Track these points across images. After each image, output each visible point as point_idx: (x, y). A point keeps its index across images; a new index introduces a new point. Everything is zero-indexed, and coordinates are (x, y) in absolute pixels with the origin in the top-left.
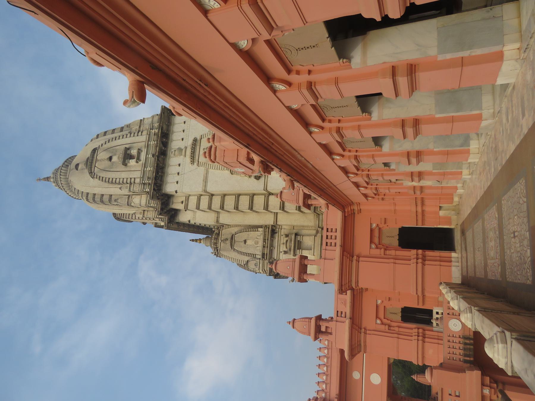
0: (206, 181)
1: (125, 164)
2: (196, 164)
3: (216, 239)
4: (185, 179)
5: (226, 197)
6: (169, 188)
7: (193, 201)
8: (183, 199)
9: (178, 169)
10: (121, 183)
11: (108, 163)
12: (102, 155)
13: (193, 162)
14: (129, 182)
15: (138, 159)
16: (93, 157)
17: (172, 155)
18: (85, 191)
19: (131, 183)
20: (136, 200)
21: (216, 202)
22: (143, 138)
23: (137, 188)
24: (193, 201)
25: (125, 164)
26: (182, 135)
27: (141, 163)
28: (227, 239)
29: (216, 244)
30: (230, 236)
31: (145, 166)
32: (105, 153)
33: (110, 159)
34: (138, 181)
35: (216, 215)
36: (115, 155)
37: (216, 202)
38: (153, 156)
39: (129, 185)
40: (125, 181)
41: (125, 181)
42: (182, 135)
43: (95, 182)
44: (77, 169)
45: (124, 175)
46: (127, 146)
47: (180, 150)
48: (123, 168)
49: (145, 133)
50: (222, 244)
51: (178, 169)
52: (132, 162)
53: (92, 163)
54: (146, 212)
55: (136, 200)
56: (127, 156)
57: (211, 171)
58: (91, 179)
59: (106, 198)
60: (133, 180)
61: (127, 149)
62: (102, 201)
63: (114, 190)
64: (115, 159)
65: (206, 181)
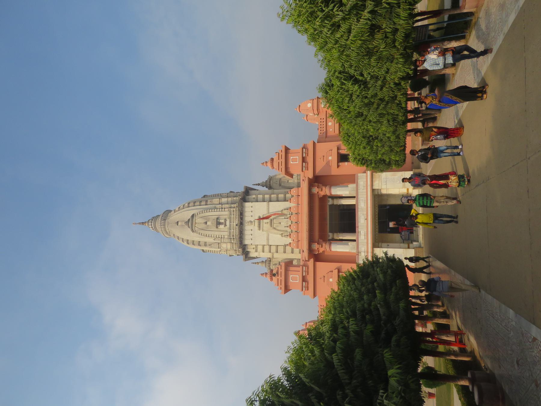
0: (268, 239)
1: (217, 227)
2: (261, 230)
3: (270, 264)
4: (255, 237)
6: (247, 242)
7: (260, 248)
8: (254, 247)
9: (251, 232)
10: (216, 238)
11: (204, 225)
12: (198, 220)
13: (259, 229)
14: (220, 237)
15: (225, 225)
16: (192, 221)
17: (246, 224)
18: (185, 238)
20: (224, 246)
21: (273, 249)
22: (227, 213)
23: (226, 241)
24: (260, 248)
25: (217, 227)
26: (251, 214)
28: (276, 264)
29: (269, 266)
30: (277, 263)
31: (230, 229)
32: (201, 219)
33: (206, 223)
34: (227, 237)
37: (273, 249)
38: (237, 225)
40: (218, 236)
41: (218, 236)
42: (251, 214)
43: (195, 234)
45: (217, 233)
46: (217, 217)
47: (251, 222)
48: (217, 230)
50: (273, 267)
51: (251, 232)
52: (222, 227)
53: (192, 224)
55: (224, 246)
56: (218, 223)
57: (270, 234)
60: (223, 236)
61: (217, 219)
62: (199, 245)
63: (210, 240)
64: (209, 223)
65: (268, 239)
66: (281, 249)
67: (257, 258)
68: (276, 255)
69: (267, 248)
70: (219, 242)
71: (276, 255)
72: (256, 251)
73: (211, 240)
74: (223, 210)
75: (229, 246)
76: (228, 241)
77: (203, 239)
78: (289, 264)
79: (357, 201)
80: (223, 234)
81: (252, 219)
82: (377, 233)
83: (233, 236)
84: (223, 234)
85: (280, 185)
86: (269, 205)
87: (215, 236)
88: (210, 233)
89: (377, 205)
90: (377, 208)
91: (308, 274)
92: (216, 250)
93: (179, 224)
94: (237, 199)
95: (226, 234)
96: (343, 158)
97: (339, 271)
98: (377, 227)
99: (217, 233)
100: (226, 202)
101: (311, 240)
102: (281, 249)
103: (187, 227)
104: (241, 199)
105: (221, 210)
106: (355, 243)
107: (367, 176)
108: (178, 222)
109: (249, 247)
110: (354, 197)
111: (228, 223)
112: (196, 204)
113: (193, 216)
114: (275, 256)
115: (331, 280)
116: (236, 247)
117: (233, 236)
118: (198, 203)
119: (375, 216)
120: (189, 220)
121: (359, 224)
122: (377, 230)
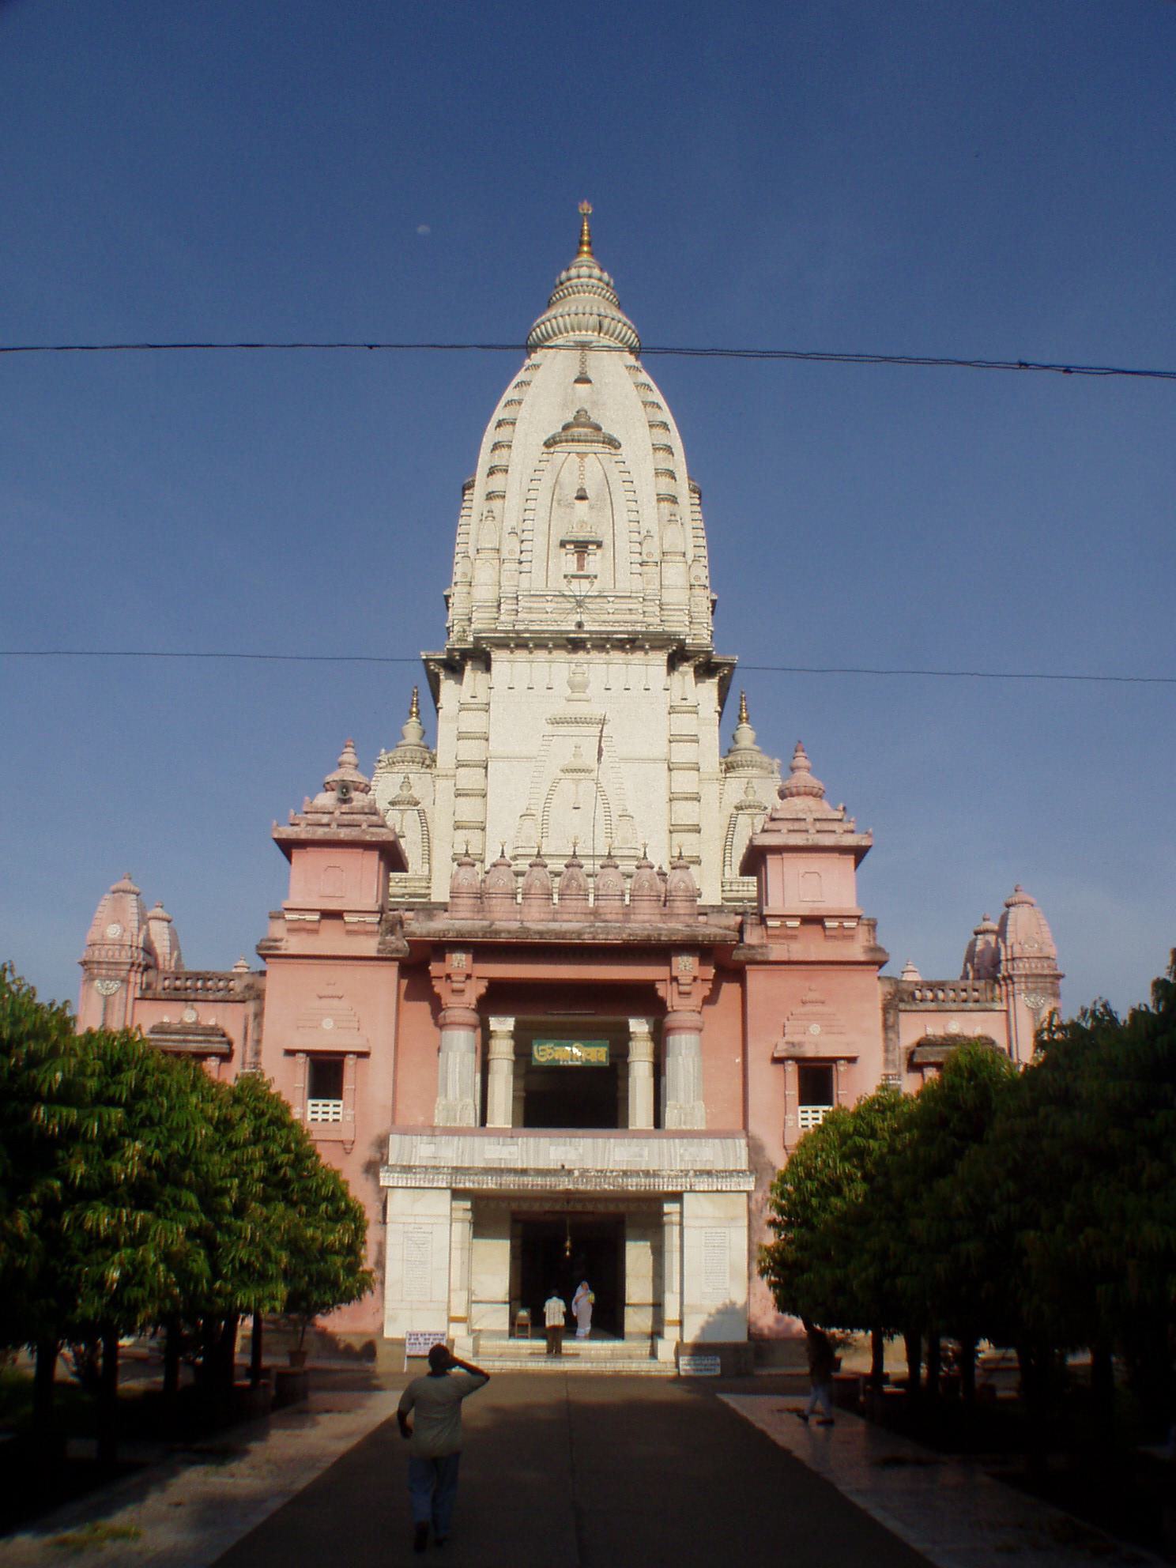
1: (563, 544)
2: (550, 729)
5: (479, 800)
7: (472, 722)
12: (594, 466)
13: (555, 722)
19: (521, 563)
21: (469, 778)
24: (472, 722)
27: (563, 585)
30: (416, 793)
33: (582, 497)
34: (525, 585)
35: (451, 772)
36: (591, 507)
37: (469, 778)
39: (517, 556)
41: (526, 546)
44: (577, 381)
45: (538, 544)
46: (607, 541)
47: (584, 686)
49: (637, 583)
50: (400, 778)
52: (570, 562)
54: (466, 589)
58: (545, 438)
59: (497, 482)
60: (525, 567)
61: (599, 545)
66: (468, 809)
67: (437, 711)
68: (445, 787)
69: (471, 750)
70: (505, 554)
71: (445, 787)
72: (463, 707)
73: (511, 520)
74: (637, 568)
75: (484, 593)
76: (508, 589)
77: (513, 484)
78: (392, 857)
79: (640, 1134)
80: (537, 567)
81: (594, 689)
82: (514, 1206)
83: (530, 610)
84: (537, 567)
85: (738, 808)
86: (655, 760)
87: (526, 535)
88: (543, 513)
89: (622, 1208)
90: (612, 1208)
91: (349, 933)
92: (472, 539)
93: (582, 388)
94: (678, 625)
95: (534, 581)
96: (816, 1079)
97: (363, 1055)
98: (536, 1207)
99: (538, 544)
100: (665, 582)
101: (485, 950)
102: (468, 809)
103: (569, 418)
104: (682, 644)
105: (637, 558)
106: (471, 1119)
107: (730, 1173)
108: (588, 381)
109: (481, 676)
110: (658, 1122)
111: (581, 587)
112: (661, 454)
113: (612, 443)
114: (441, 784)
115: (328, 1024)
116: (481, 622)
117: (530, 610)
118: (664, 466)
119: (580, 1200)
120: (598, 428)
121: (544, 1142)
122: (525, 1207)
